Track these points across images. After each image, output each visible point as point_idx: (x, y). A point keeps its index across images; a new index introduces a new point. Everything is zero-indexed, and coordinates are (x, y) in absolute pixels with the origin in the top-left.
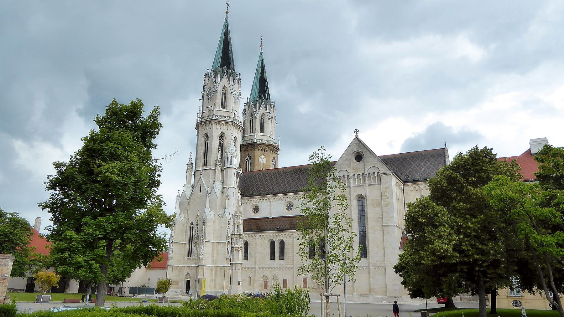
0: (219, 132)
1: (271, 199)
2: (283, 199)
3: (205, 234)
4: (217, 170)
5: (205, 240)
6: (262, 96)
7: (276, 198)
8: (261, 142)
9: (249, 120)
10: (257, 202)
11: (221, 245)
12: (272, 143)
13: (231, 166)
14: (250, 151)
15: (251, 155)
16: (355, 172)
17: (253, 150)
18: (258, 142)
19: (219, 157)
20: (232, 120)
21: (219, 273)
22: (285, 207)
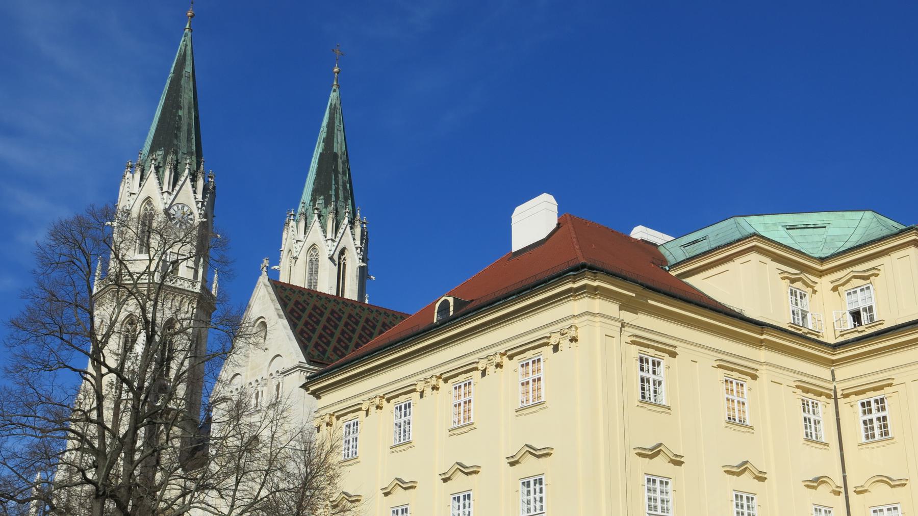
6: (320, 201)
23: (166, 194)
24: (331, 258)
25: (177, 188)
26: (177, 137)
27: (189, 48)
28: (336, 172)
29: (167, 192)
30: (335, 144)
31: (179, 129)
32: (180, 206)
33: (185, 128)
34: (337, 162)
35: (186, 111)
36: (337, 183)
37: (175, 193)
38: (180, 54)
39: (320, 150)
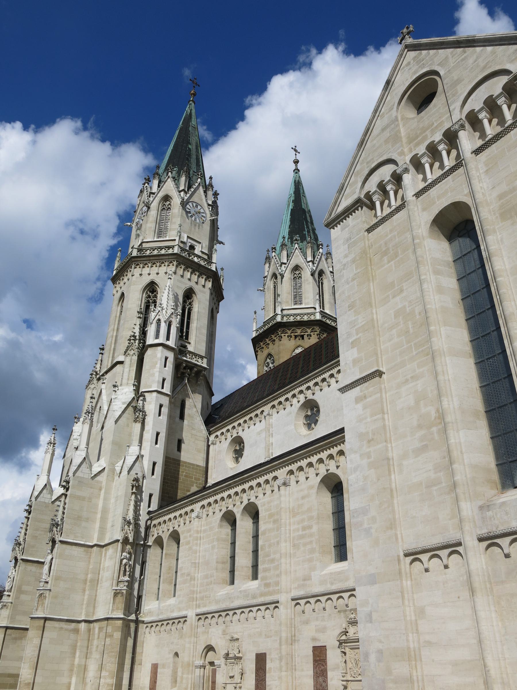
0: (146, 280)
1: (267, 409)
2: (295, 401)
3: (62, 519)
4: (127, 360)
5: (58, 538)
6: (297, 237)
7: (276, 403)
8: (292, 319)
9: (272, 287)
10: (240, 428)
11: (110, 550)
12: (318, 317)
13: (157, 341)
14: (271, 345)
15: (273, 353)
16: (418, 144)
17: (277, 340)
18: (285, 320)
19: (137, 331)
20: (176, 250)
21: (95, 642)
22: (302, 421)
23: (182, 193)
24: (312, 275)
25: (192, 190)
26: (188, 159)
27: (193, 111)
28: (307, 222)
29: (183, 190)
30: (303, 204)
31: (189, 155)
32: (195, 205)
33: (194, 157)
34: (306, 215)
35: (194, 147)
36: (308, 227)
37: (190, 192)
38: (187, 114)
39: (291, 207)
